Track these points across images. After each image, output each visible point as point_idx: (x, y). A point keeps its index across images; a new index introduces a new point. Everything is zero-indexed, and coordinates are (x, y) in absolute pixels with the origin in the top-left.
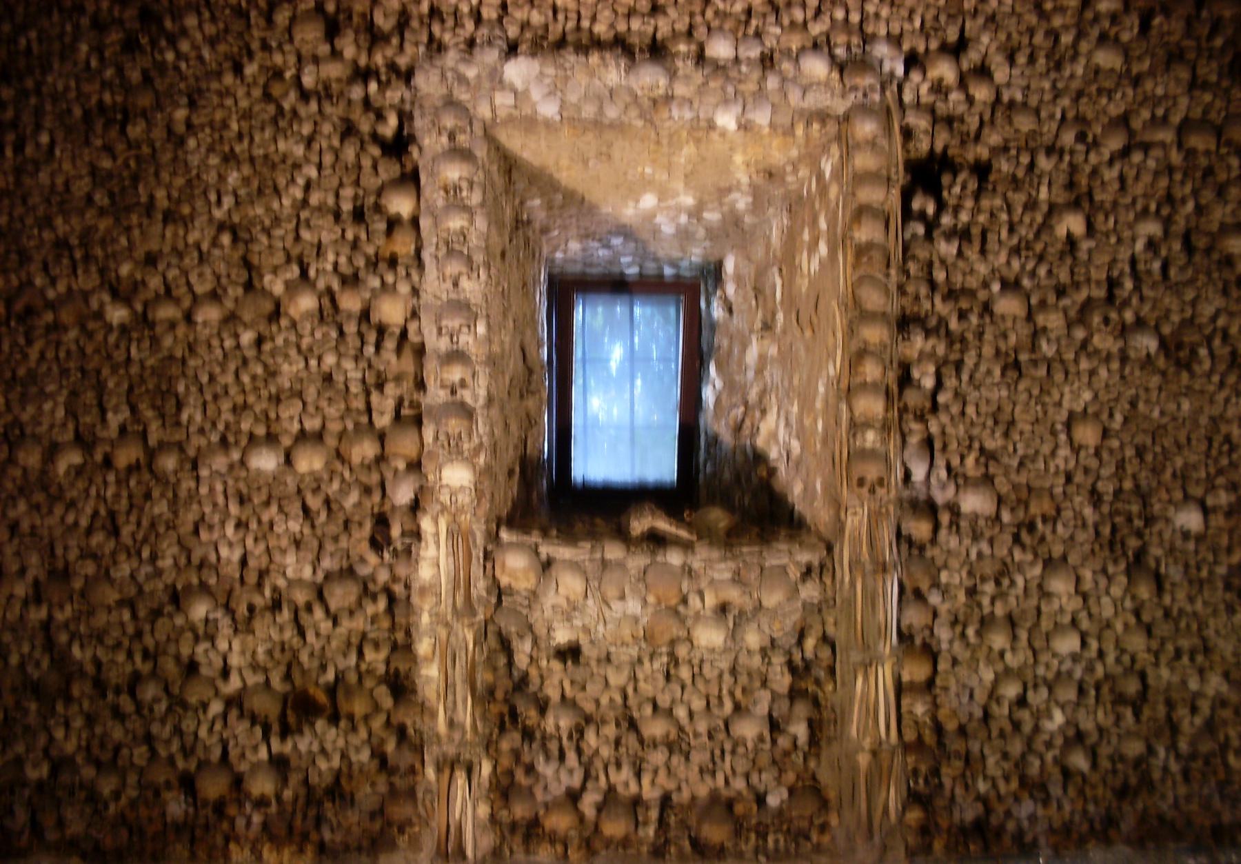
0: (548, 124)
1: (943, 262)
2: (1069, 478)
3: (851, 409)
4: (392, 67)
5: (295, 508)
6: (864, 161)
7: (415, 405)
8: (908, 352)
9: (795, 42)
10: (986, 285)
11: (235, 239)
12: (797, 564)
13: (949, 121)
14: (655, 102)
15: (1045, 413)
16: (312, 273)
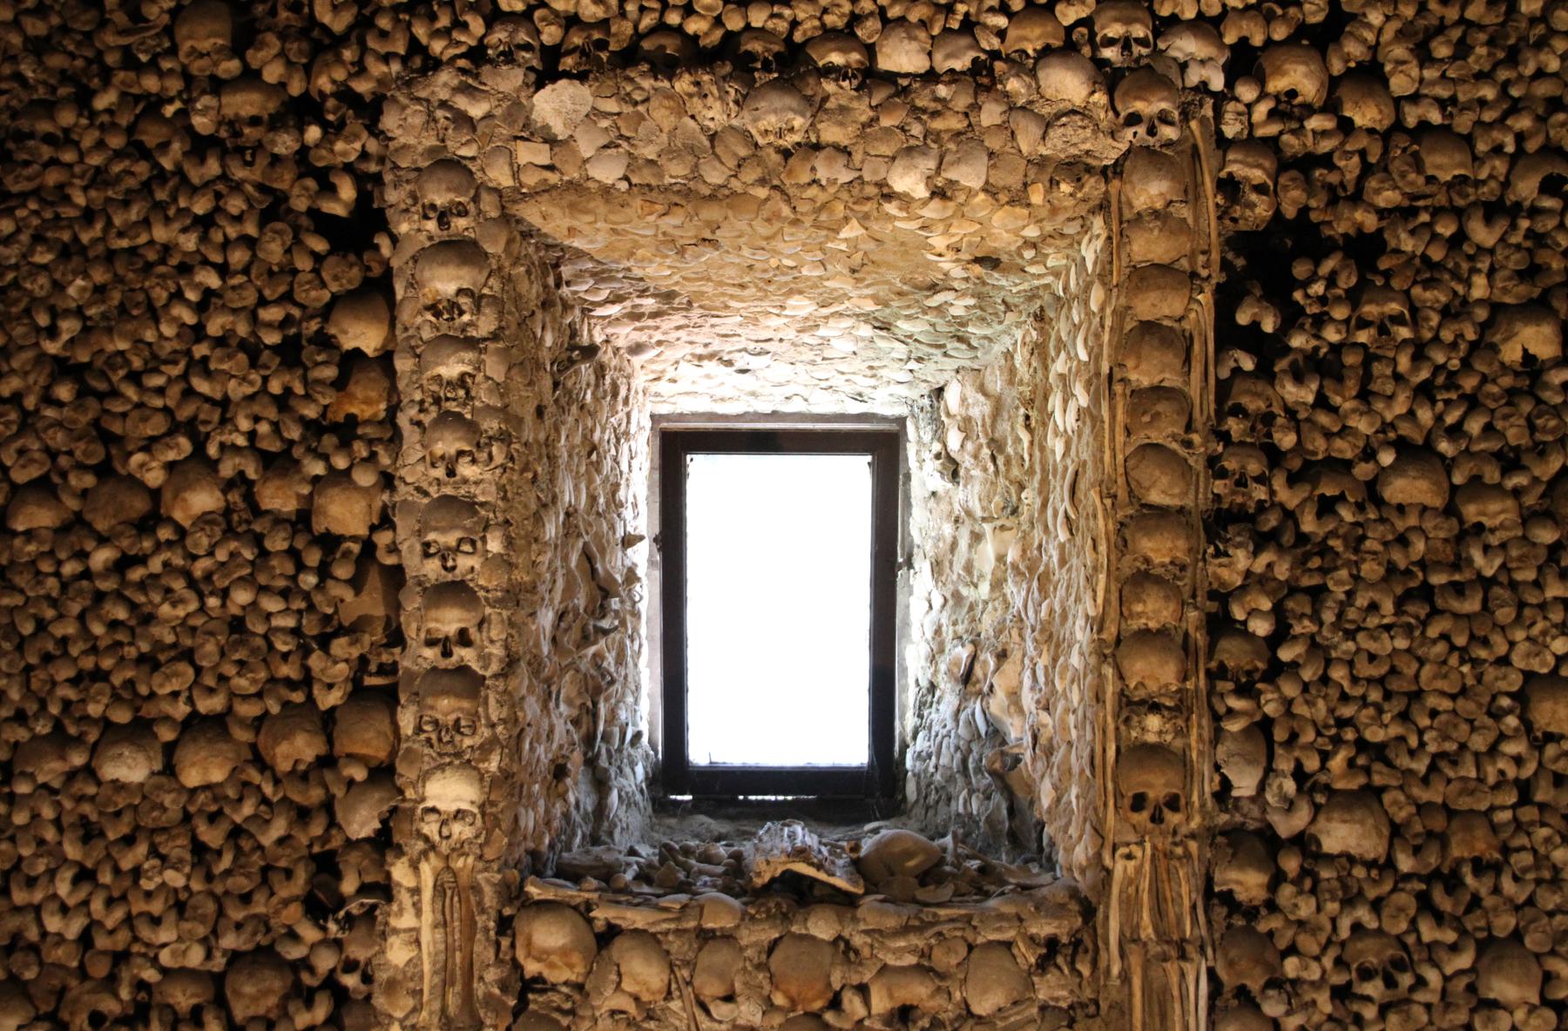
0: (606, 191)
1: (1291, 413)
2: (1525, 789)
3: (1121, 677)
4: (346, 95)
5: (177, 848)
6: (1148, 247)
7: (389, 669)
8: (1225, 574)
9: (1031, 38)
10: (1369, 454)
11: (83, 392)
12: (1032, 939)
13: (1306, 164)
14: (786, 154)
15: (1479, 679)
16: (212, 450)
